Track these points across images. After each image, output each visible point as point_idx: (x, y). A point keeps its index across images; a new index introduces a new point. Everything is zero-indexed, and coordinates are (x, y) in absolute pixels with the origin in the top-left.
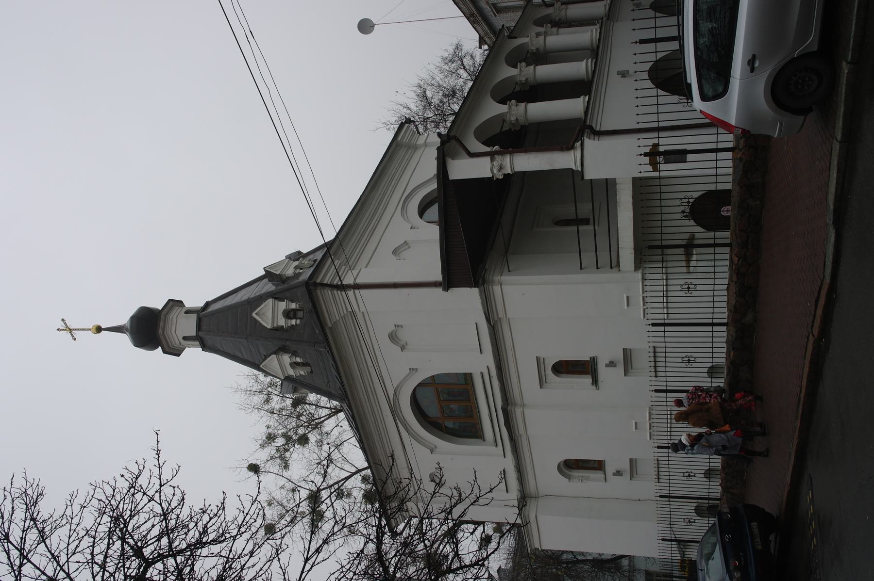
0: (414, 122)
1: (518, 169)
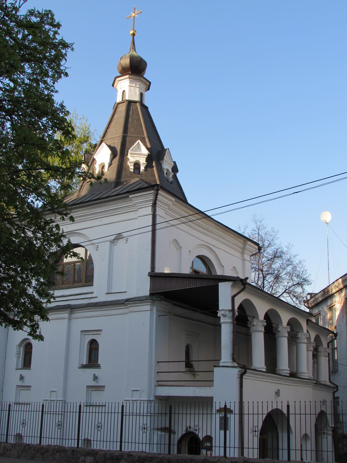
0: (259, 252)
1: (223, 326)
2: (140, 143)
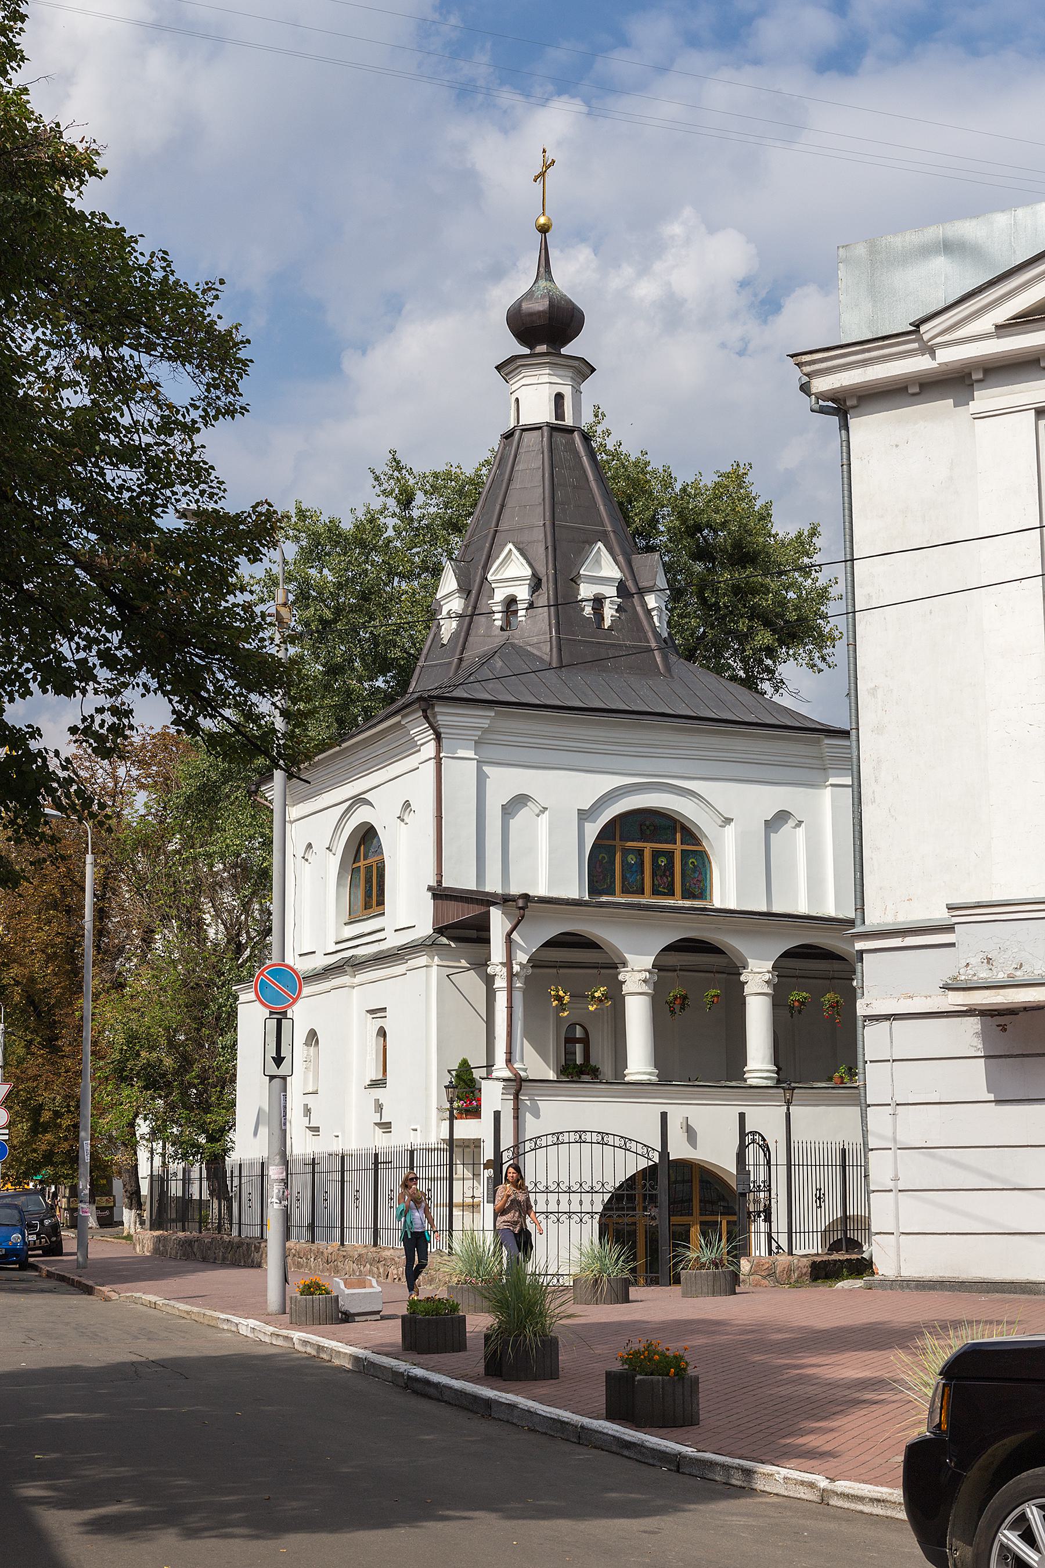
2: (514, 550)
